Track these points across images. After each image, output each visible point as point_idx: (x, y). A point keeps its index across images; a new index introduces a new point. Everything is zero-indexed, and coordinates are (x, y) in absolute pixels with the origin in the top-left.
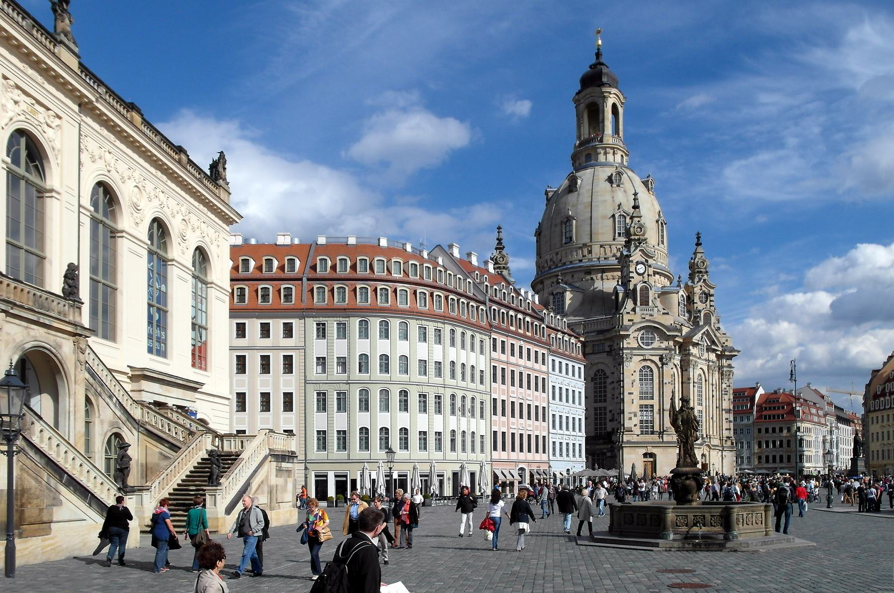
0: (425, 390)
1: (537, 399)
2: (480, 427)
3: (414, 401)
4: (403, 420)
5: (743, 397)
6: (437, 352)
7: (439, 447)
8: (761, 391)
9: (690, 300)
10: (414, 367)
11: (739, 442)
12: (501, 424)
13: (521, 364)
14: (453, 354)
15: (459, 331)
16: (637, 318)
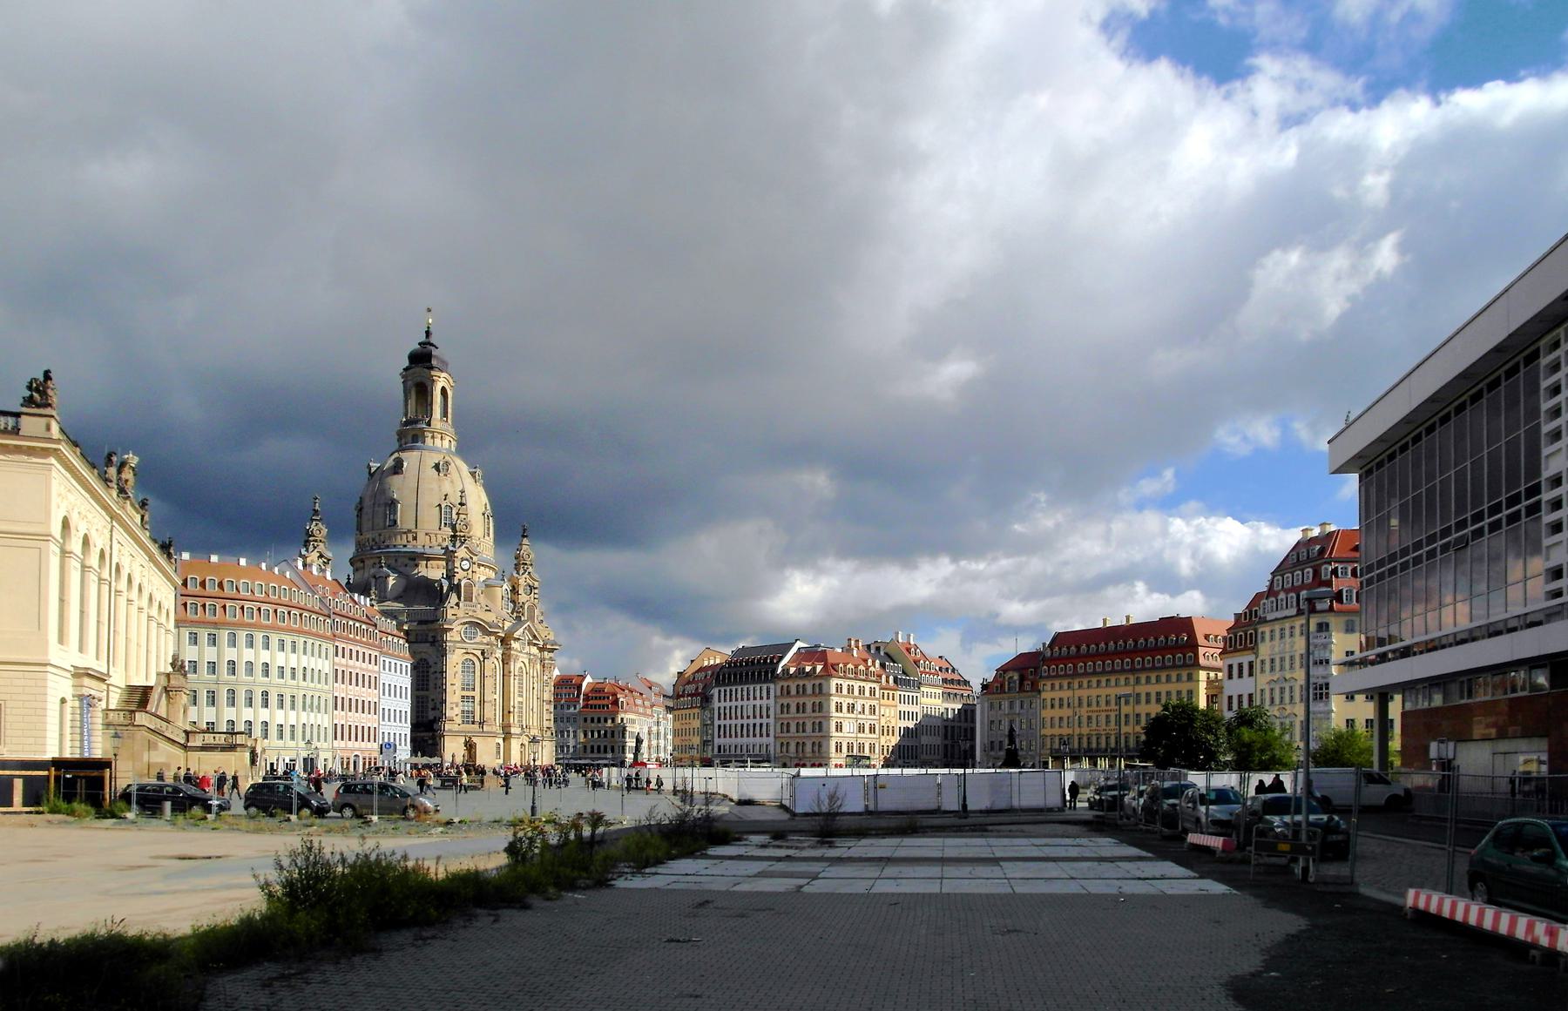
0: (282, 691)
1: (368, 695)
2: (324, 720)
3: (273, 699)
4: (264, 714)
5: (566, 686)
6: (293, 660)
7: (293, 738)
8: (588, 679)
9: (514, 590)
10: (274, 672)
11: (560, 732)
12: (341, 717)
13: (357, 666)
14: (305, 661)
15: (310, 642)
16: (460, 613)
